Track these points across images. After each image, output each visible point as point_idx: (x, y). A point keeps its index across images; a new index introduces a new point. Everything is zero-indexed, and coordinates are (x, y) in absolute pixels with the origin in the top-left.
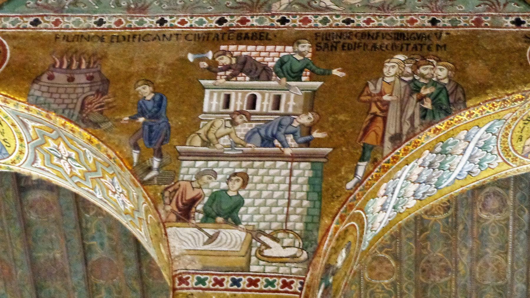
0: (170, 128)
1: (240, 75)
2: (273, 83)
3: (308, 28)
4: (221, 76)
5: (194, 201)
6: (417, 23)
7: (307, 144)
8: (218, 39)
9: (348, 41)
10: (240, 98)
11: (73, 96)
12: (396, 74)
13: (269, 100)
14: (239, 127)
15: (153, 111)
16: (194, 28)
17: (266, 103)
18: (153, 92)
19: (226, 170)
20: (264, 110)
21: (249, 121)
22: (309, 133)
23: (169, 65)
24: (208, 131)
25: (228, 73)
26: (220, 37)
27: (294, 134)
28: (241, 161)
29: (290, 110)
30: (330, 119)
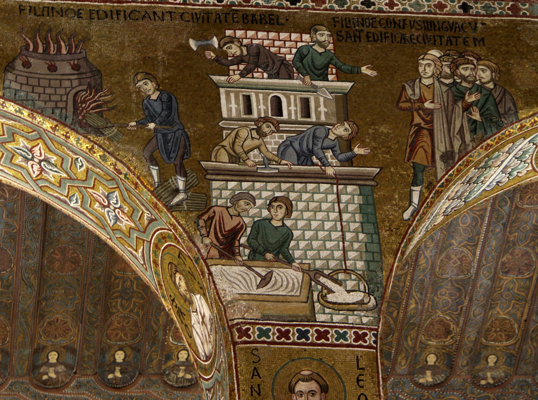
0: (188, 137)
1: (256, 70)
2: (296, 82)
3: (324, 10)
4: (234, 71)
5: (236, 232)
6: (448, 9)
7: (350, 162)
8: (221, 22)
9: (373, 30)
10: (261, 101)
11: (61, 91)
12: (433, 74)
13: (296, 105)
14: (268, 139)
15: (164, 113)
16: (188, 5)
17: (293, 108)
18: (158, 90)
19: (265, 194)
20: (293, 117)
21: (278, 131)
22: (351, 150)
23: (169, 54)
24: (234, 143)
25: (242, 67)
26: (223, 17)
27: (332, 148)
28: (280, 182)
29: (323, 118)
30: (370, 131)
